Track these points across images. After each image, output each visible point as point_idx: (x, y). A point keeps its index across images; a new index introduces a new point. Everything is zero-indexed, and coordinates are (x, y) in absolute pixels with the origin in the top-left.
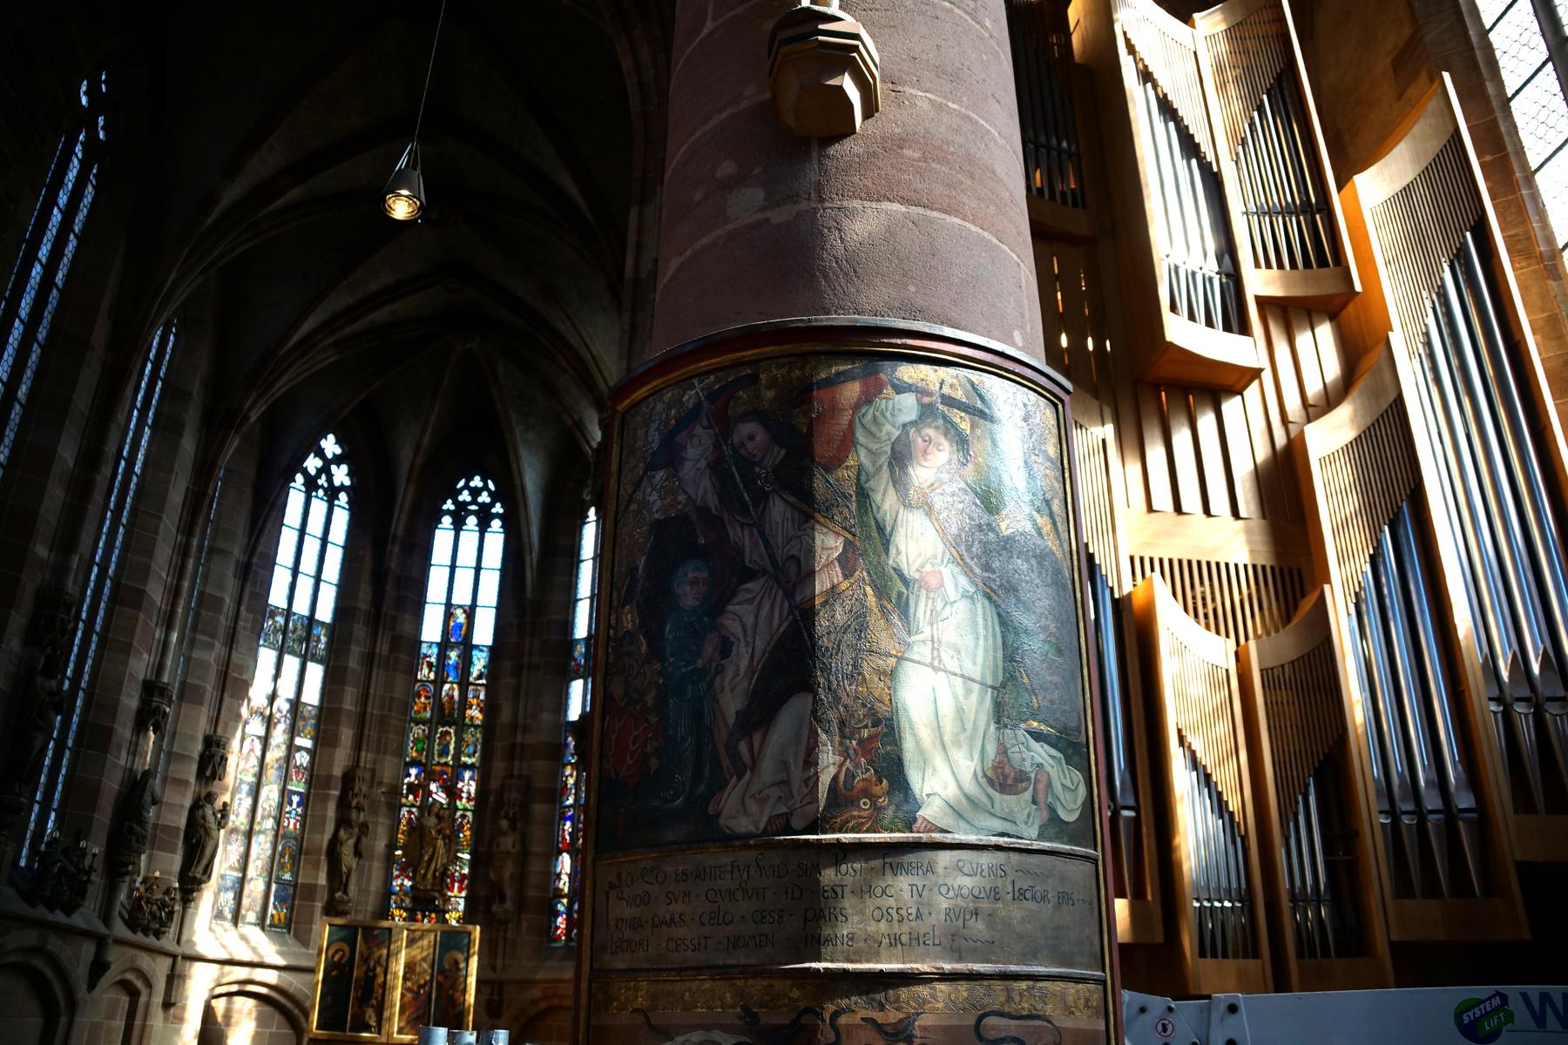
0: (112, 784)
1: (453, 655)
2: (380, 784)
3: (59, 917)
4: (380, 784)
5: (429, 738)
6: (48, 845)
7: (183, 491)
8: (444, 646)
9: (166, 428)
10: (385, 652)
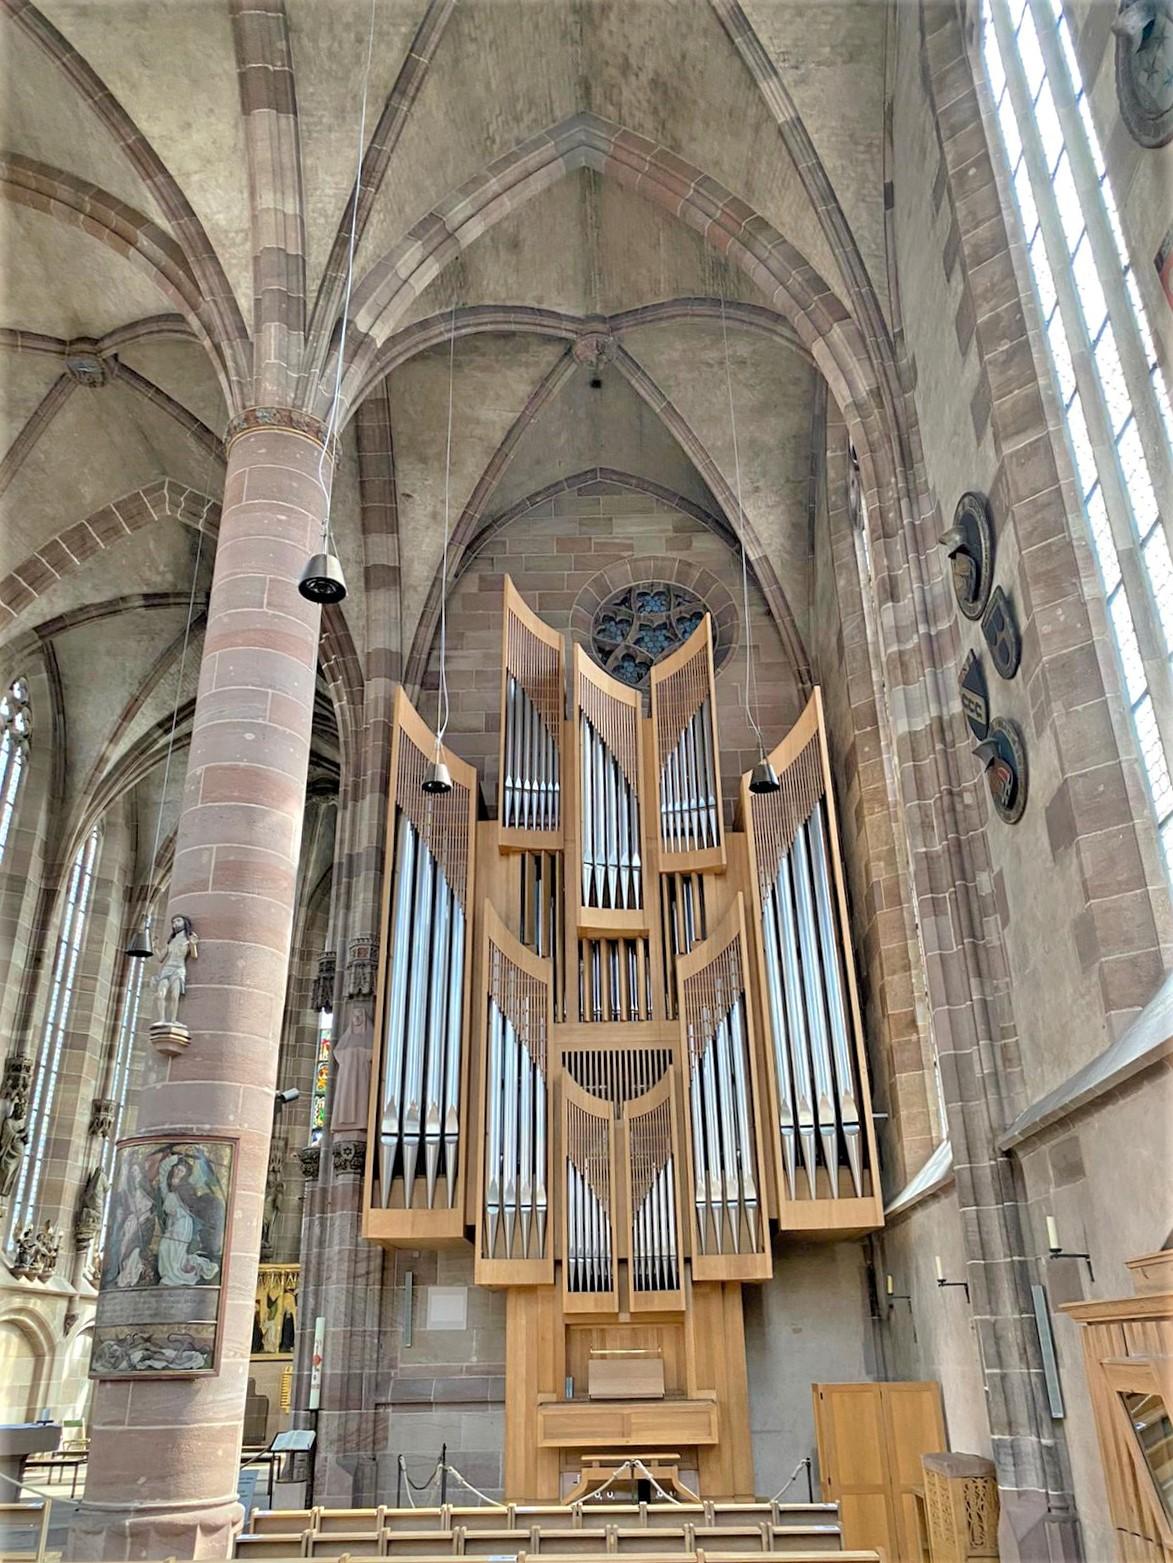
0: (72, 1182)
2: (292, 1149)
3: (37, 1284)
4: (292, 1149)
6: (26, 1234)
7: (113, 953)
9: (98, 911)
10: (292, 1042)
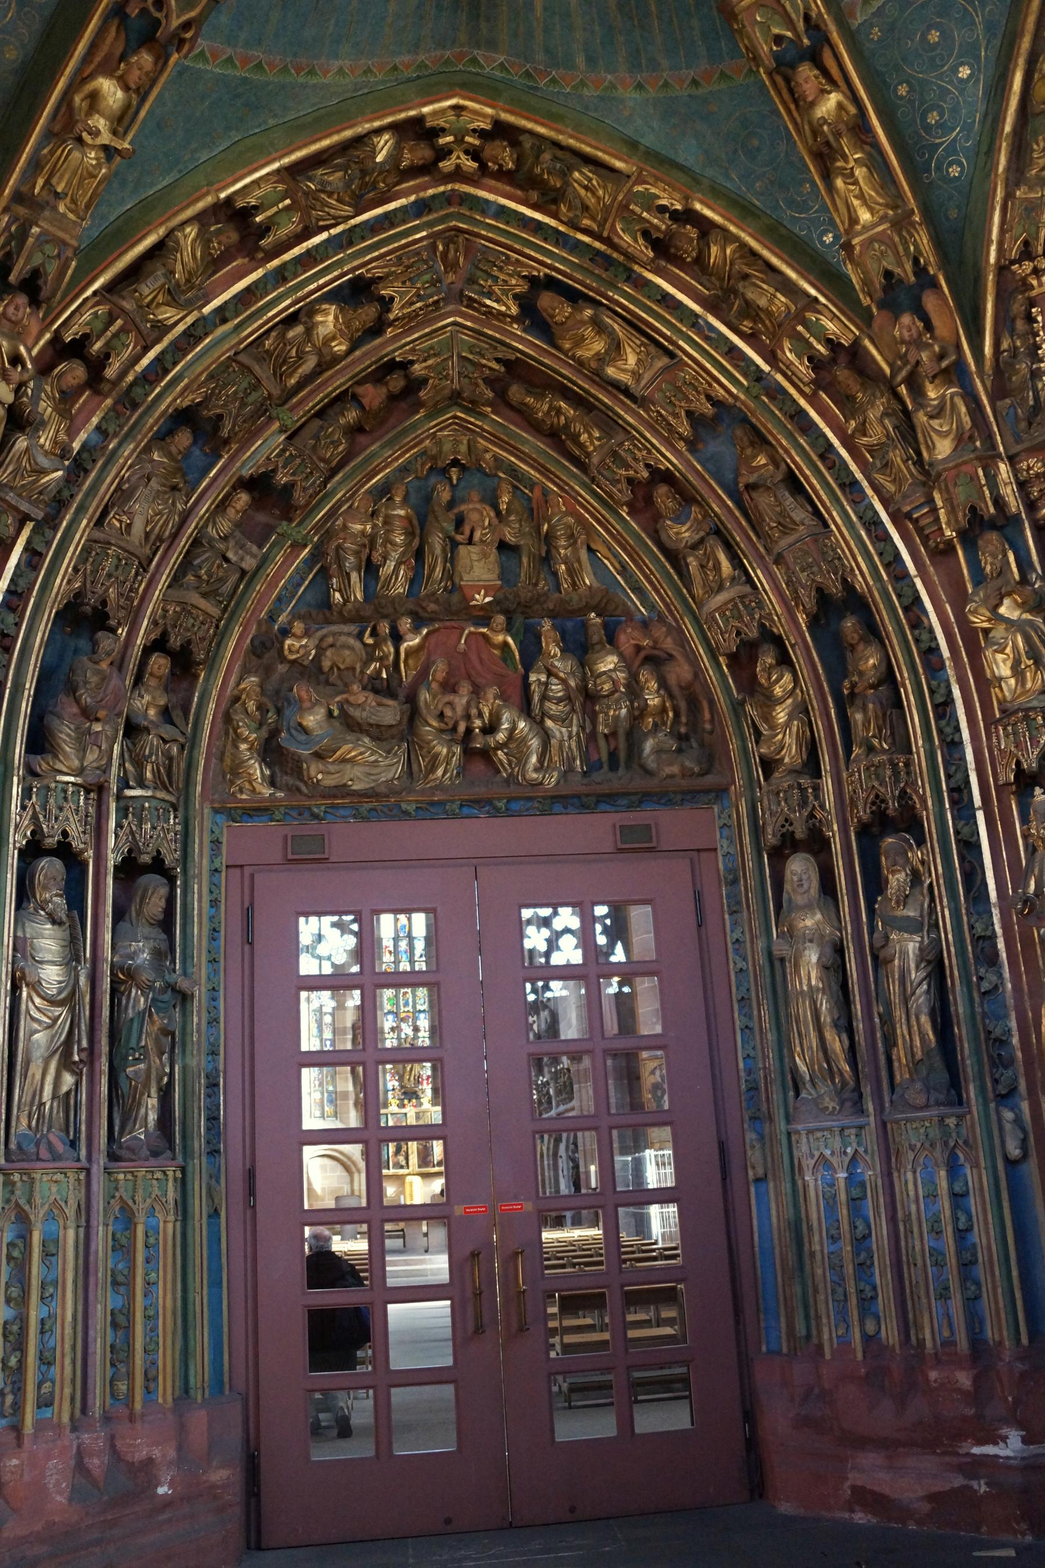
1: (403, 945)
5: (396, 996)
8: (396, 939)
